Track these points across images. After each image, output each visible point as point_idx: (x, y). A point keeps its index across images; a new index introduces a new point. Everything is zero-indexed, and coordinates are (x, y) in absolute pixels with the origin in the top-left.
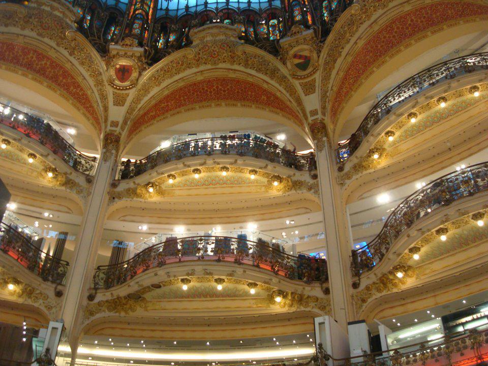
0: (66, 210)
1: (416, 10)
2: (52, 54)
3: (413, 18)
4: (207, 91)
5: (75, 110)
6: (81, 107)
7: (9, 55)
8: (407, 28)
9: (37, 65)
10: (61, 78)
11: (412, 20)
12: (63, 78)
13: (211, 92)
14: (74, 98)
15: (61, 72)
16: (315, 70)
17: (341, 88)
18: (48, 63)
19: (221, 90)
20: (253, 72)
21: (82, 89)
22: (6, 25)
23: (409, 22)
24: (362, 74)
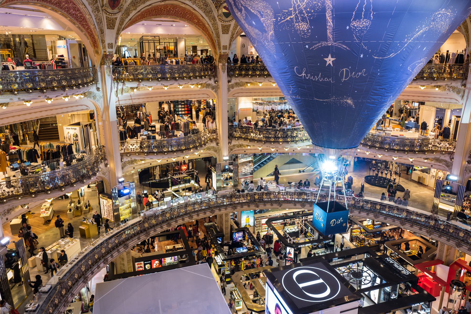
4: (162, 10)
13: (164, 11)
19: (171, 10)
20: (197, 8)
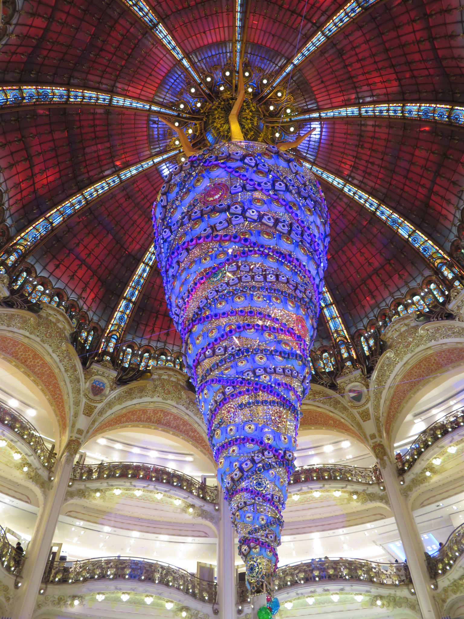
0: (204, 534)
1: (437, 353)
2: (174, 411)
3: (436, 358)
5: (195, 449)
6: (199, 446)
7: (144, 417)
8: (432, 365)
9: (164, 420)
10: (182, 427)
11: (435, 360)
12: (184, 426)
14: (193, 440)
15: (182, 422)
16: (368, 401)
17: (389, 413)
18: (172, 417)
21: (198, 433)
22: (141, 397)
23: (433, 361)
24: (403, 400)
